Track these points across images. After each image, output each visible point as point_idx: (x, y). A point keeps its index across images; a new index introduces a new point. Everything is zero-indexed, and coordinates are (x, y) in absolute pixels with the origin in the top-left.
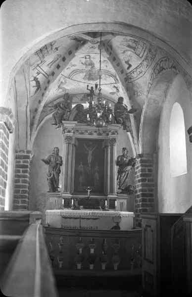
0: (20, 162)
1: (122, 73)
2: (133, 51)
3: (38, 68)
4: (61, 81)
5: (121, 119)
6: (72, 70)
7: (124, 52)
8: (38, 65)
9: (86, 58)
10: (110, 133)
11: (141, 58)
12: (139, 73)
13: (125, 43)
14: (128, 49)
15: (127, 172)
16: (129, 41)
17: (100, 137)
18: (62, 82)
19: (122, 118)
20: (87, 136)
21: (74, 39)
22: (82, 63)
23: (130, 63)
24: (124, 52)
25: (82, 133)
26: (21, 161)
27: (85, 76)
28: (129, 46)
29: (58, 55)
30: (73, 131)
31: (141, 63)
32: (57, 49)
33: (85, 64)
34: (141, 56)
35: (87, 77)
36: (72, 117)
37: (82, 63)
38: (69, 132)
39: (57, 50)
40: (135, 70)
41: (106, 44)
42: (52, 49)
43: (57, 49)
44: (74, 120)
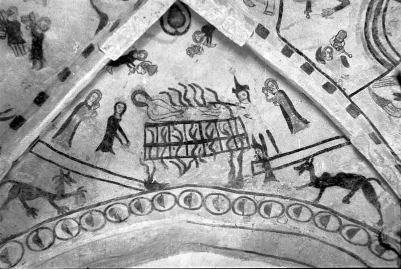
3: (274, 164)
4: (391, 97)
6: (361, 48)
29: (266, 89)
32: (239, 88)
39: (245, 88)
42: (228, 105)
43: (239, 88)
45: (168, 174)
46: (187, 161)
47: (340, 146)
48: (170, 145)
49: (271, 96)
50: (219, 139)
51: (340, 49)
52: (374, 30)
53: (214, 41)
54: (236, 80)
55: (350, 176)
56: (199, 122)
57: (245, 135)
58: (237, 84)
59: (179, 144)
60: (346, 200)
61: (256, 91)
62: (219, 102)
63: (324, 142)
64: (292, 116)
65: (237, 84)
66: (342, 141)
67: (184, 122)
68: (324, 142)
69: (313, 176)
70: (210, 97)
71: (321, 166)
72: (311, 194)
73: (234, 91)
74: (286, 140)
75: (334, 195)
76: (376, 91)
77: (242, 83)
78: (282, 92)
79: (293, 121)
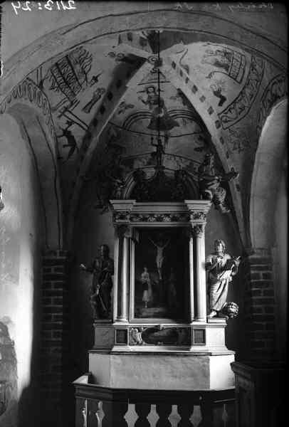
0: (49, 270)
1: (210, 113)
2: (224, 71)
3: (67, 113)
5: (210, 192)
7: (210, 76)
8: (66, 109)
9: (148, 92)
10: (192, 216)
11: (240, 83)
12: (239, 110)
13: (211, 59)
14: (216, 69)
15: (224, 282)
16: (216, 54)
17: (175, 224)
18: (113, 137)
19: (212, 190)
20: (153, 224)
21: (122, 60)
22: (143, 101)
23: (223, 94)
24: (210, 76)
25: (145, 219)
26: (53, 268)
27: (151, 122)
28: (217, 64)
29: (99, 89)
30: (128, 217)
31: (241, 93)
32: (95, 79)
33: (149, 102)
34: (239, 79)
35: (154, 124)
36: (127, 192)
37: (143, 101)
38: (122, 217)
40: (232, 106)
41: (178, 64)
42: (86, 79)
43: (95, 79)
44: (131, 197)
45: (47, 85)
46: (56, 85)
47: (84, 129)
48: (60, 71)
49: (96, 93)
50: (70, 88)
51: (126, 108)
52: (137, 116)
53: (120, 62)
54: (99, 75)
55: (75, 141)
56: (75, 74)
57: (75, 95)
58: (97, 77)
59: (62, 75)
60: (65, 146)
61: (97, 85)
62: (86, 74)
63: (83, 122)
64: (90, 105)
65: (97, 77)
66: (86, 128)
67: (73, 69)
68: (83, 122)
69: (66, 129)
70: (86, 70)
71: (73, 129)
72: (61, 133)
73: (94, 77)
74: (78, 111)
75: (65, 140)
76: (112, 128)
77: (98, 78)
78: (100, 96)
79: (87, 108)
